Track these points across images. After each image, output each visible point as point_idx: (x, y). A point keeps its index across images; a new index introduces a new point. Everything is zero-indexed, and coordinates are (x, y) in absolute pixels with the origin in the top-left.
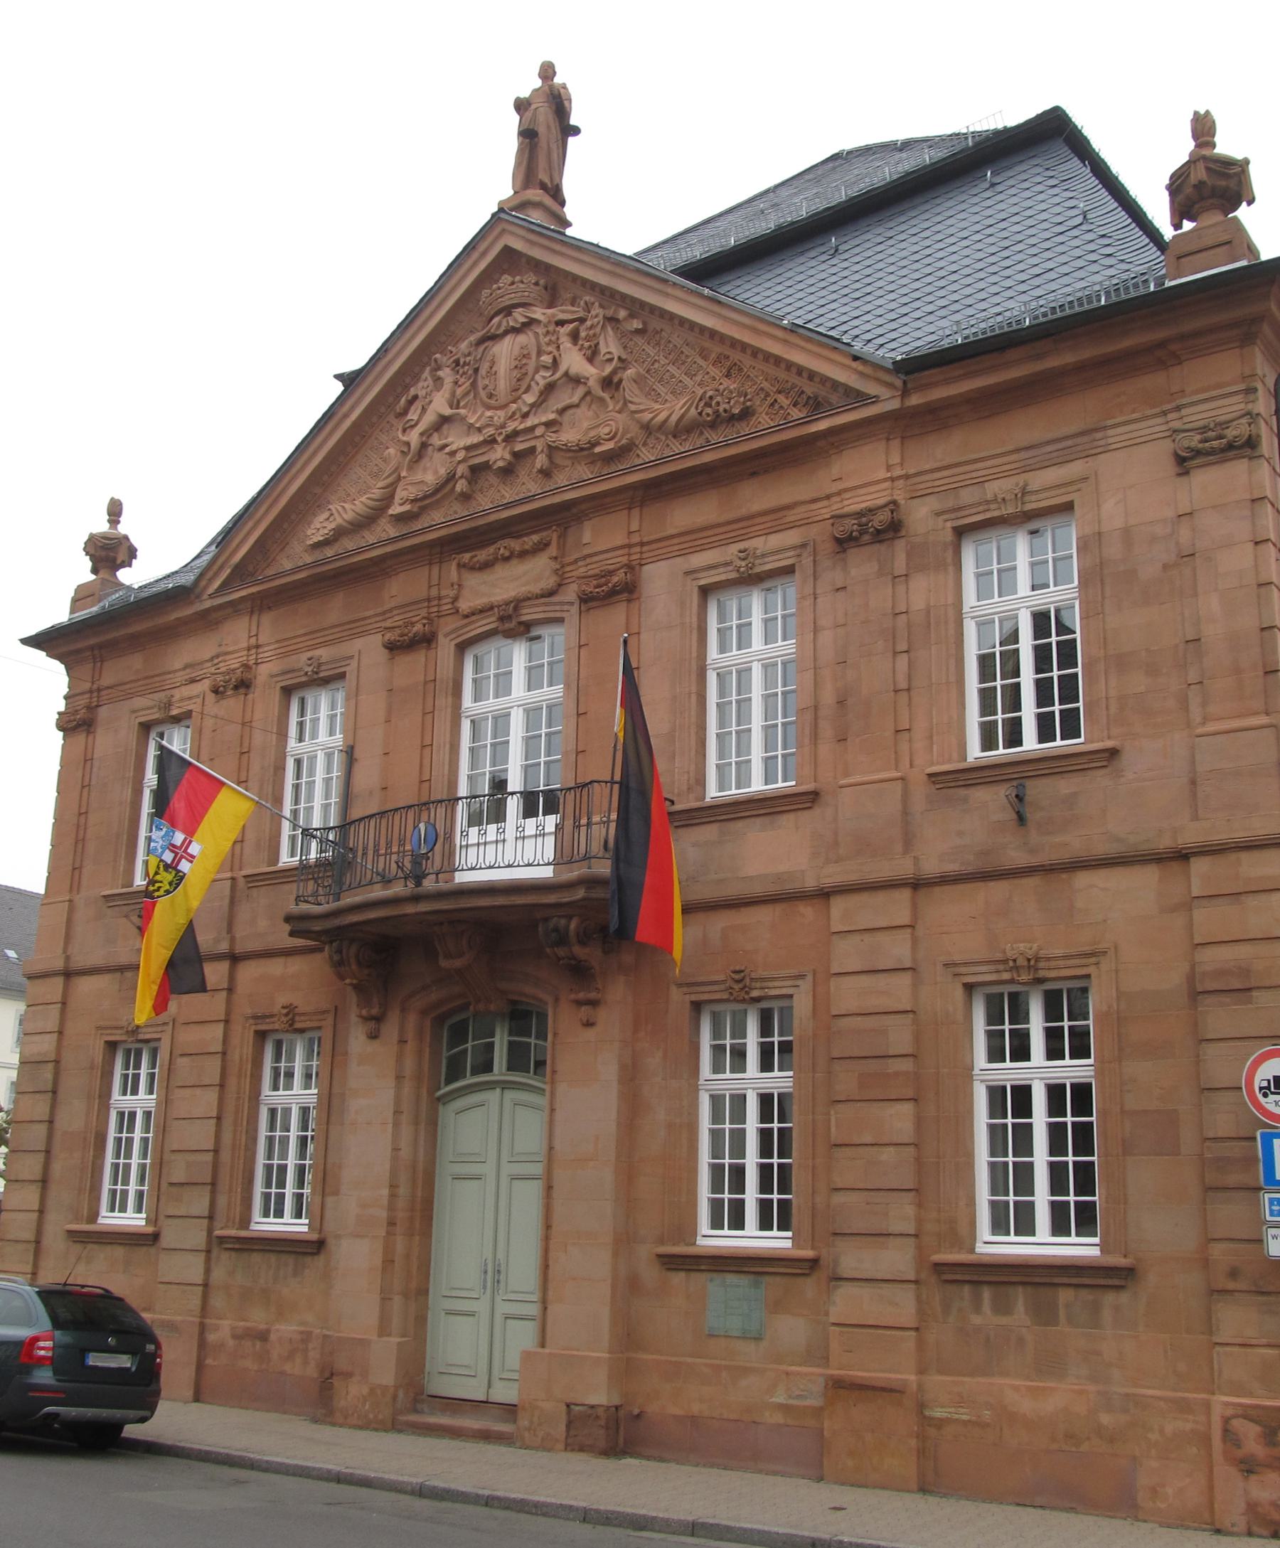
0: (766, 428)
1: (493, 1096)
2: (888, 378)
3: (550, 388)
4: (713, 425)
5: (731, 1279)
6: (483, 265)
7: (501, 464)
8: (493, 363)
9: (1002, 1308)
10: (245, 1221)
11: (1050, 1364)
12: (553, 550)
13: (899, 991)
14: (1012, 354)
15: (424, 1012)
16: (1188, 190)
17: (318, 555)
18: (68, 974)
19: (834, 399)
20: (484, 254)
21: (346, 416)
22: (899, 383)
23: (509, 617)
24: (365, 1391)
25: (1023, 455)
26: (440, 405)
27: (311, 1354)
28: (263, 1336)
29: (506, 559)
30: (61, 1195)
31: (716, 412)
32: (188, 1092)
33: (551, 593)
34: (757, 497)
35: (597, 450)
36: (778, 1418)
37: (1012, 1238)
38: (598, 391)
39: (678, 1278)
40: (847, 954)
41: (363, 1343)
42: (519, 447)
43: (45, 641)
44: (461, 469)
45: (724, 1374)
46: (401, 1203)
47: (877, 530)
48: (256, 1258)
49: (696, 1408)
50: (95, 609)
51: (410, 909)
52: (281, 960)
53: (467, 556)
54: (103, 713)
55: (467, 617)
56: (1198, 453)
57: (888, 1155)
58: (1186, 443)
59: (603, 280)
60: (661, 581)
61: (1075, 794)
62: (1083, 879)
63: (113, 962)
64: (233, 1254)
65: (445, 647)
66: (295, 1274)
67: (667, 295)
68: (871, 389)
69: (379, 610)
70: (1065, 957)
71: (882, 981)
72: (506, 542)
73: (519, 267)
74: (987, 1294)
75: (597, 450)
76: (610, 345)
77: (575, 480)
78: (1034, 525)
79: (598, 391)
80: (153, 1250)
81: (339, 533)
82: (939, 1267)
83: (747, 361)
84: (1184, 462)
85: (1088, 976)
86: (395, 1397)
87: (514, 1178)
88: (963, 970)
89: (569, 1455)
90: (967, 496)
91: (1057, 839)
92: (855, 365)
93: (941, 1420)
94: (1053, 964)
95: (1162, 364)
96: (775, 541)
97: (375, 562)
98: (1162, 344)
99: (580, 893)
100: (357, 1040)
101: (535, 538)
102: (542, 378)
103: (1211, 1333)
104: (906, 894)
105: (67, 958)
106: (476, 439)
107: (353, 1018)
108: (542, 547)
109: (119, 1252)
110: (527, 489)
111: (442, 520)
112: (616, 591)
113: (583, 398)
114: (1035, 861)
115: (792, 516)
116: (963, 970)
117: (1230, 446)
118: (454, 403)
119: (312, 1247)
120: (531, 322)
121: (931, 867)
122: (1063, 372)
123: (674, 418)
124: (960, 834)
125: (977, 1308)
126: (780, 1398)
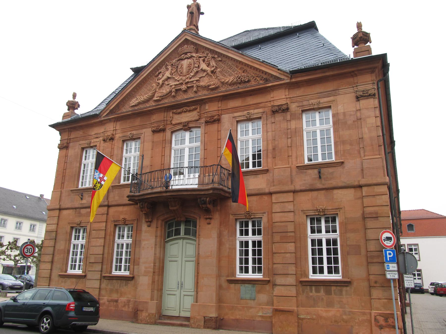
0: (253, 85)
1: (180, 241)
2: (287, 75)
3: (197, 72)
4: (240, 83)
5: (246, 285)
6: (180, 42)
7: (184, 89)
8: (182, 65)
9: (317, 291)
10: (111, 272)
11: (330, 304)
12: (198, 110)
13: (290, 217)
14: (318, 71)
15: (163, 221)
16: (358, 38)
17: (133, 109)
18: (60, 209)
19: (271, 79)
20: (180, 40)
21: (142, 75)
22: (290, 76)
23: (186, 126)
24: (147, 315)
25: (319, 95)
26: (168, 74)
27: (130, 305)
28: (117, 301)
29: (185, 112)
30: (57, 265)
31: (241, 81)
32: (95, 239)
33: (197, 120)
34: (251, 101)
35: (210, 87)
36: (260, 319)
37: (318, 275)
38: (210, 73)
39: (232, 285)
40: (276, 208)
41: (146, 303)
42: (189, 86)
43: (54, 126)
44: (173, 90)
45: (245, 309)
46: (157, 267)
48: (114, 281)
49: (238, 317)
50: (69, 119)
51: (164, 194)
53: (175, 111)
54: (71, 144)
55: (174, 125)
56: (362, 96)
58: (359, 94)
59: (212, 48)
60: (226, 119)
61: (333, 172)
62: (335, 191)
63: (73, 206)
64: (108, 280)
65: (168, 132)
66: (125, 285)
67: (229, 52)
68: (282, 77)
69: (150, 122)
70: (331, 209)
71: (286, 214)
72: (185, 108)
73: (189, 43)
74: (313, 288)
75: (210, 87)
76: (213, 63)
77: (203, 95)
78: (319, 111)
79: (210, 73)
80: (84, 279)
81: (139, 104)
82: (301, 282)
83: (248, 69)
84: (358, 98)
85: (337, 214)
86: (155, 316)
87: (186, 261)
88: (306, 212)
89: (205, 329)
90: (305, 103)
91: (330, 182)
92: (278, 71)
93: (303, 318)
94: (329, 211)
95: (352, 76)
96: (256, 111)
97: (149, 111)
98: (353, 72)
99: (211, 192)
100: (144, 227)
101: (194, 107)
102: (195, 70)
103: (371, 296)
104: (291, 194)
105: (60, 205)
106: (177, 83)
107: (144, 221)
108: (195, 109)
109: (74, 280)
110: (190, 95)
111: (168, 102)
112: (214, 121)
113: (206, 75)
114: (324, 187)
115: (261, 105)
116: (306, 212)
117: (370, 95)
118: (171, 74)
119: (130, 279)
120: (192, 57)
121: (298, 188)
122: (329, 76)
123: (230, 81)
124: (305, 180)
125: (311, 292)
126: (260, 314)
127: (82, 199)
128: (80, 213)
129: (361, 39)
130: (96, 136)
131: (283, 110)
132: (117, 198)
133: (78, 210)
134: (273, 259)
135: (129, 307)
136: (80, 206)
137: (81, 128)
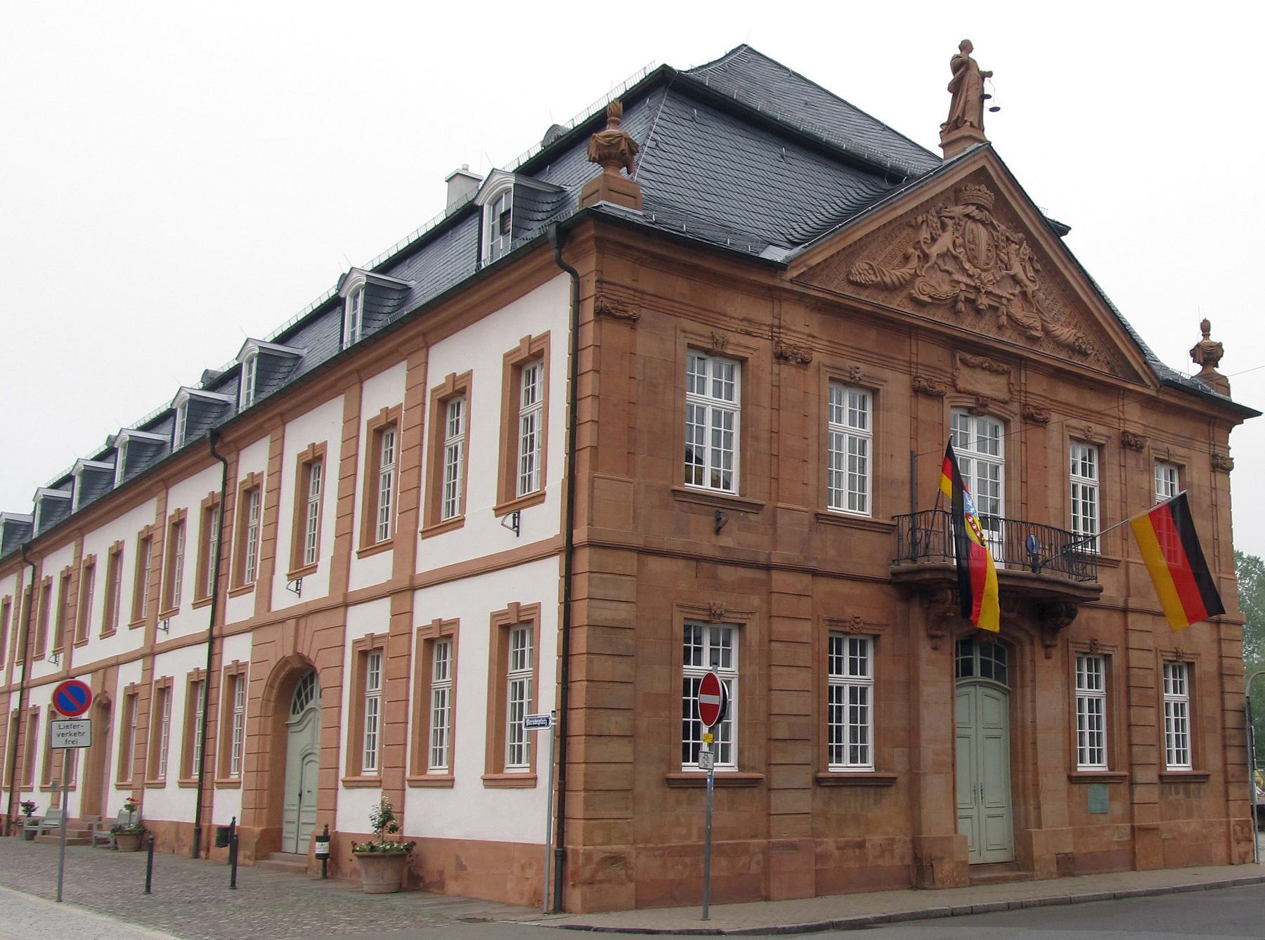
17: (848, 291)
34: (1094, 402)
47: (1129, 443)
53: (968, 357)
57: (1149, 730)
59: (1036, 234)
68: (1148, 382)
97: (911, 326)
101: (1005, 367)
108: (1007, 373)
112: (1035, 419)
115: (1107, 419)
128: (714, 577)
129: (1208, 354)
130: (743, 326)
131: (1129, 443)
132: (831, 553)
134: (1130, 737)
136: (718, 554)
137: (691, 272)
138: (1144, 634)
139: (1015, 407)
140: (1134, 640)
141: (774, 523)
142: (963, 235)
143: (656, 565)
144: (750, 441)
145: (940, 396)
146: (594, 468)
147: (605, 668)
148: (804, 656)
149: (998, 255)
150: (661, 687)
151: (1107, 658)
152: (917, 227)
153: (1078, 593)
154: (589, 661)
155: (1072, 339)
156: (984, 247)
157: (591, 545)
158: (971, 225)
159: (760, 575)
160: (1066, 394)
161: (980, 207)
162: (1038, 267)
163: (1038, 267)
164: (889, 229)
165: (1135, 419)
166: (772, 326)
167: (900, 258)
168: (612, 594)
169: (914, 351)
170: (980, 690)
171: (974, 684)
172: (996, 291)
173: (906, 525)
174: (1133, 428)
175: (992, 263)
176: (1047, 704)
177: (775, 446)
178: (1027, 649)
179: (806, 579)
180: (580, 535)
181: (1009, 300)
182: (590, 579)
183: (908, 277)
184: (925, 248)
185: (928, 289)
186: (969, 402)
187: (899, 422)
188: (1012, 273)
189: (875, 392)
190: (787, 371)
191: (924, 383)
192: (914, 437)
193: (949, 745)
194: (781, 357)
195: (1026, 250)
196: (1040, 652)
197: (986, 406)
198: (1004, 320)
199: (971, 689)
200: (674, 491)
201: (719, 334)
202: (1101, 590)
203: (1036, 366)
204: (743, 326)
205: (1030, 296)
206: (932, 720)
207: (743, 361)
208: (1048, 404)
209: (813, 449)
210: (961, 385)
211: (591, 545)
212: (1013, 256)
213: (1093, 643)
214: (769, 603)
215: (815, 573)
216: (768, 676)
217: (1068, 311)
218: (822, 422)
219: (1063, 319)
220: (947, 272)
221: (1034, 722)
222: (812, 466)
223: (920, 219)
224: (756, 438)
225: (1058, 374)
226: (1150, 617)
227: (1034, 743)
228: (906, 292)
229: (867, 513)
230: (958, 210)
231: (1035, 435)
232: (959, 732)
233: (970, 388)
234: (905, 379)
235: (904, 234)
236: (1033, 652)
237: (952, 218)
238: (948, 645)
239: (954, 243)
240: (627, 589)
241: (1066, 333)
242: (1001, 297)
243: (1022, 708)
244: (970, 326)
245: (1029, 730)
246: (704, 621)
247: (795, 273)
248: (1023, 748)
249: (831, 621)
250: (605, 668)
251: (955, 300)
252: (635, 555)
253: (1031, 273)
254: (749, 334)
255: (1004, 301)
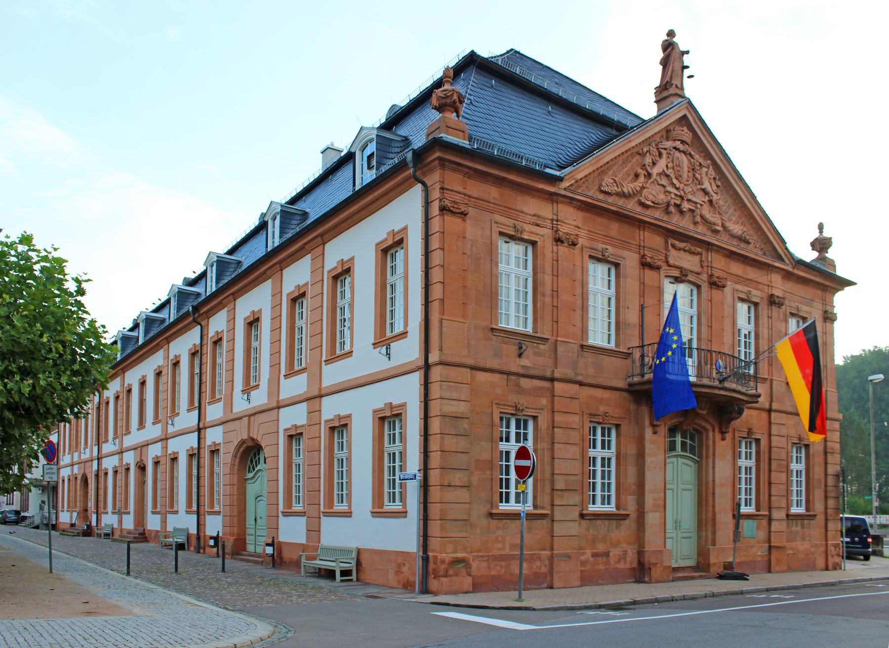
29: (685, 251)
32: (562, 446)
34: (752, 273)
48: (599, 522)
51: (717, 392)
52: (601, 390)
53: (677, 243)
66: (617, 528)
97: (641, 221)
101: (699, 250)
108: (701, 254)
112: (716, 284)
115: (760, 286)
127: (520, 355)
128: (518, 385)
130: (534, 219)
131: (773, 301)
132: (591, 371)
133: (513, 378)
135: (625, 562)
138: (782, 427)
139: (704, 277)
140: (775, 430)
141: (555, 351)
142: (673, 161)
143: (481, 376)
144: (539, 297)
145: (658, 268)
146: (442, 312)
147: (451, 443)
148: (575, 436)
149: (694, 175)
150: (486, 456)
151: (758, 441)
152: (643, 155)
153: (745, 398)
154: (442, 439)
155: (740, 233)
156: (686, 169)
157: (441, 363)
158: (677, 154)
159: (546, 384)
160: (736, 268)
161: (683, 142)
162: (719, 183)
163: (719, 183)
164: (626, 155)
165: (779, 286)
166: (552, 220)
167: (632, 176)
168: (455, 395)
169: (642, 238)
170: (680, 460)
171: (677, 456)
172: (694, 199)
173: (637, 354)
174: (777, 292)
175: (691, 181)
176: (722, 469)
177: (555, 300)
178: (711, 434)
179: (576, 387)
180: (434, 358)
181: (701, 205)
182: (441, 386)
183: (638, 189)
184: (649, 169)
185: (651, 197)
186: (676, 273)
187: (632, 285)
188: (703, 187)
189: (617, 265)
190: (563, 250)
191: (649, 260)
192: (642, 295)
193: (663, 495)
194: (558, 240)
195: (712, 172)
196: (718, 436)
197: (686, 276)
198: (698, 219)
199: (675, 459)
200: (492, 329)
201: (519, 225)
202: (759, 396)
203: (719, 249)
204: (534, 219)
205: (714, 203)
206: (652, 479)
207: (534, 243)
208: (724, 275)
209: (579, 302)
210: (671, 261)
211: (441, 363)
212: (704, 176)
213: (750, 432)
214: (553, 402)
215: (581, 384)
216: (552, 450)
217: (737, 214)
218: (584, 284)
219: (734, 219)
220: (663, 185)
221: (714, 481)
222: (579, 312)
223: (645, 150)
224: (544, 295)
225: (732, 255)
226: (785, 415)
227: (714, 494)
228: (636, 199)
229: (612, 345)
230: (669, 144)
231: (716, 293)
232: (668, 486)
233: (677, 263)
234: (637, 256)
235: (634, 160)
236: (714, 436)
237: (665, 149)
238: (663, 430)
239: (667, 166)
240: (465, 392)
241: (737, 229)
242: (696, 203)
243: (707, 472)
244: (677, 222)
245: (711, 485)
246: (512, 414)
247: (568, 184)
248: (706, 496)
249: (591, 415)
250: (451, 443)
251: (668, 204)
252: (468, 370)
253: (715, 188)
254: (538, 225)
255: (699, 206)
